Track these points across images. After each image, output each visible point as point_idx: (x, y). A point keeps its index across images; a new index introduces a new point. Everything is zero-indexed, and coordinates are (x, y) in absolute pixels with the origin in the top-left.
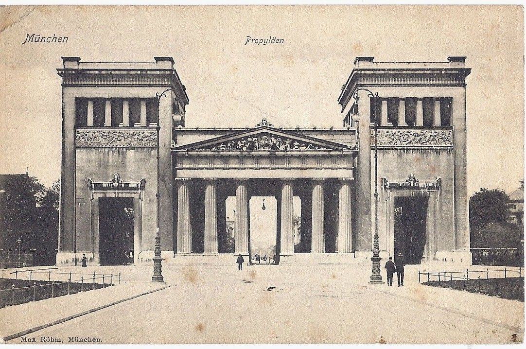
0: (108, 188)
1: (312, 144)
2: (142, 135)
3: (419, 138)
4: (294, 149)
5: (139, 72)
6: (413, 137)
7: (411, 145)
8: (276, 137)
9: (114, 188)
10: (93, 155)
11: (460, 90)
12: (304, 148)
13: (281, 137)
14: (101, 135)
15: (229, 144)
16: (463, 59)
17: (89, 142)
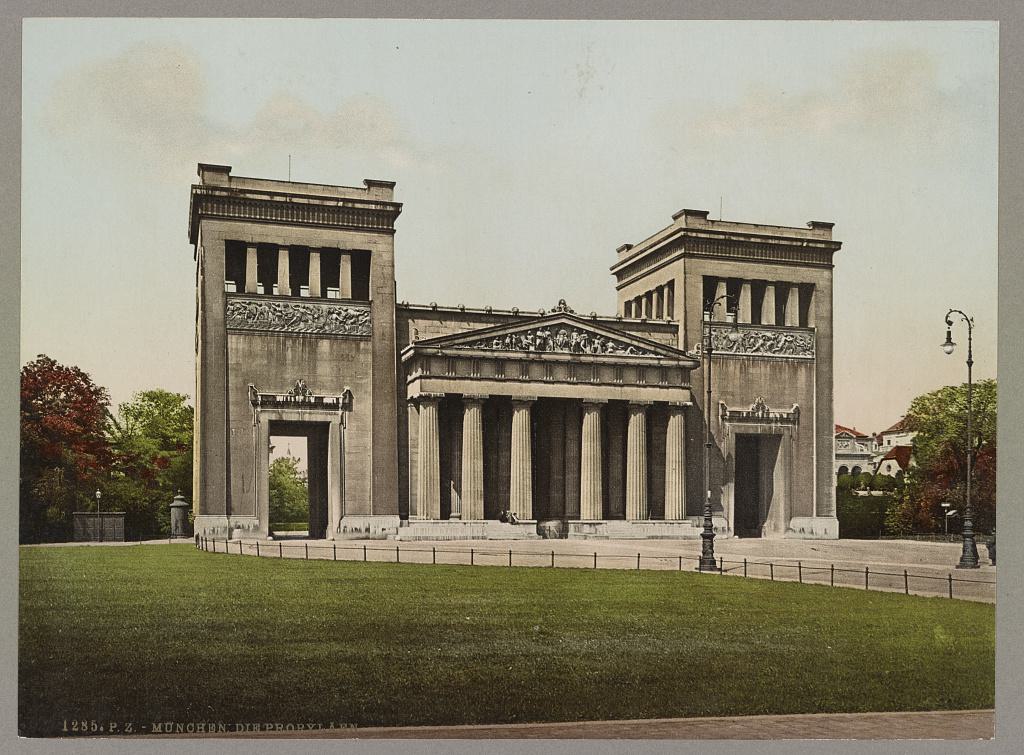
0: (285, 404)
1: (635, 346)
2: (344, 314)
3: (769, 343)
4: (607, 353)
5: (341, 204)
6: (761, 341)
7: (760, 354)
8: (580, 331)
9: (297, 405)
10: (258, 344)
11: (826, 273)
12: (620, 353)
13: (587, 332)
14: (272, 310)
15: (508, 340)
16: (829, 226)
17: (250, 321)
